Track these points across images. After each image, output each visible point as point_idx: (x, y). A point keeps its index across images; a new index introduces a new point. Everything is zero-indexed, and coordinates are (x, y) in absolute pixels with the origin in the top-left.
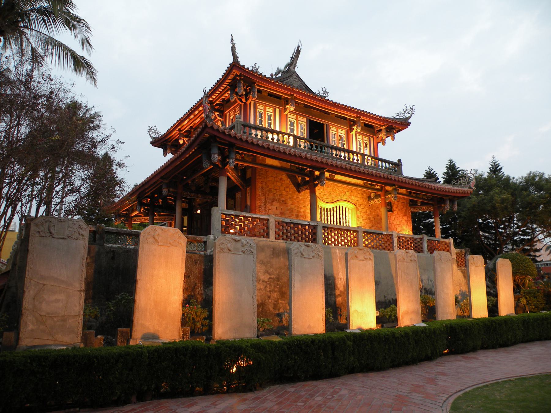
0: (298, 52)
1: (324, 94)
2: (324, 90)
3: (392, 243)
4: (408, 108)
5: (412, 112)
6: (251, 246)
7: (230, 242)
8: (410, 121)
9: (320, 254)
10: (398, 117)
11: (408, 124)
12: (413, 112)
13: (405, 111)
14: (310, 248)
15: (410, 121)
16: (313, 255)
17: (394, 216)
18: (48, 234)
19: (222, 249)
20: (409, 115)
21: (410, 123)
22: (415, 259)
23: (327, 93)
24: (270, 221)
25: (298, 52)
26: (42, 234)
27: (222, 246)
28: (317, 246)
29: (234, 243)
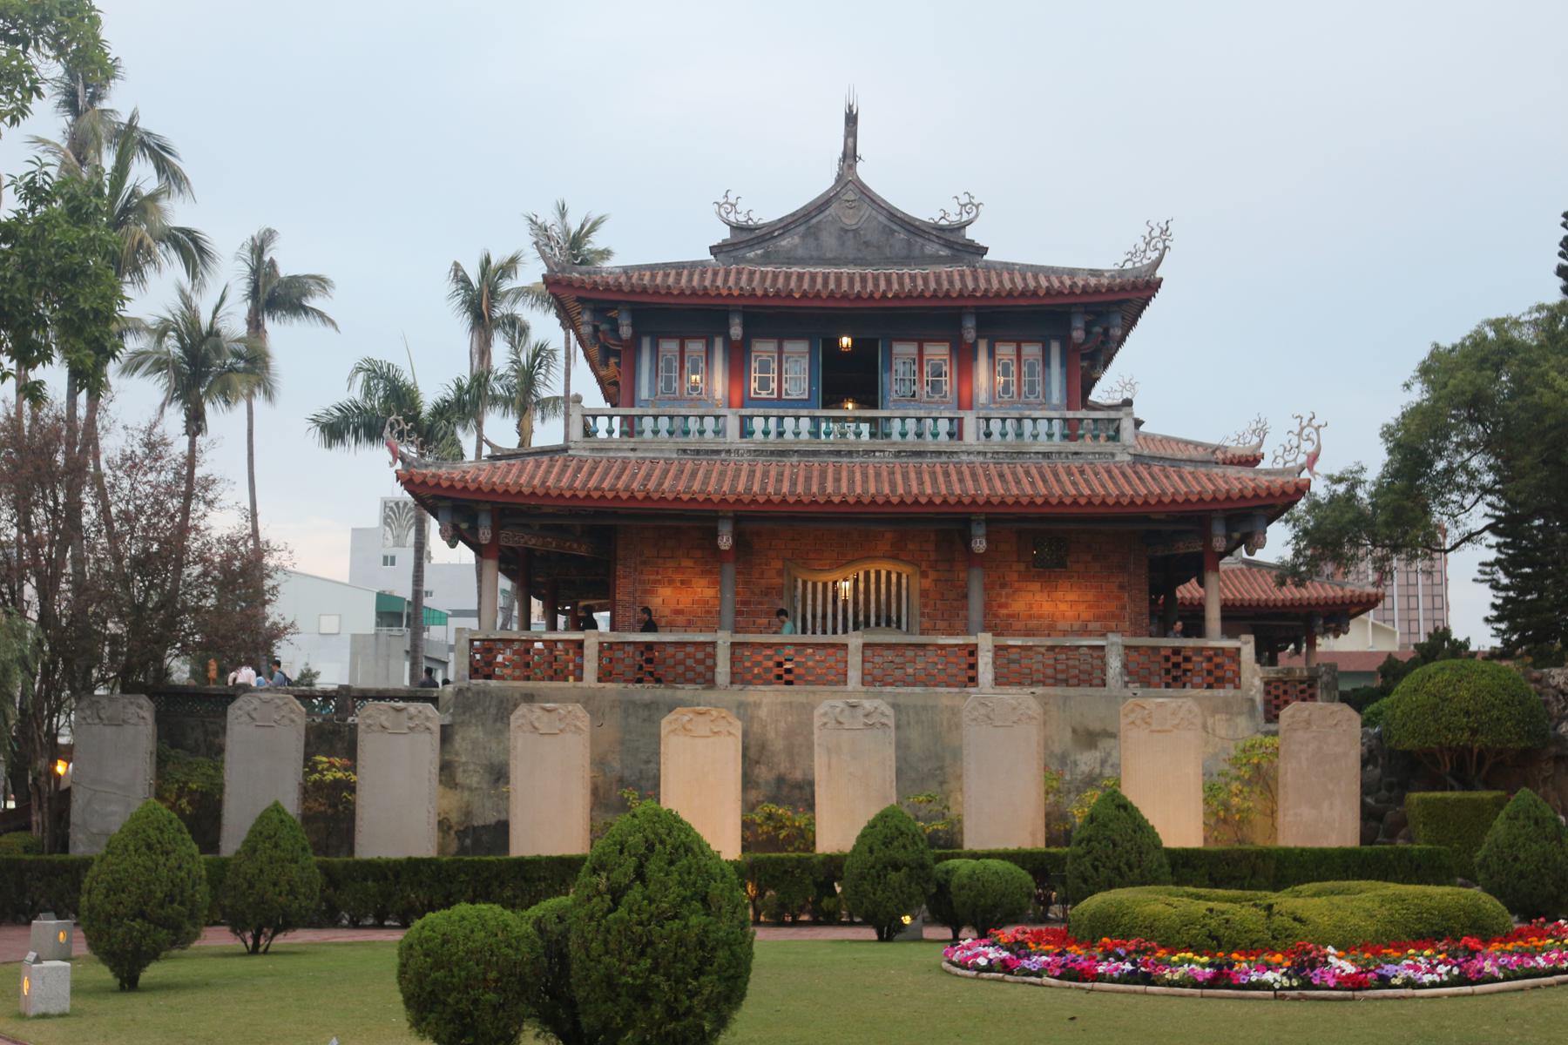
0: (851, 120)
1: (965, 214)
2: (965, 200)
3: (973, 666)
4: (1156, 233)
5: (1164, 241)
6: (428, 719)
7: (385, 712)
8: (1159, 273)
9: (578, 723)
10: (1129, 265)
11: (1159, 283)
12: (1167, 243)
13: (1148, 244)
14: (554, 715)
15: (1159, 273)
16: (562, 727)
17: (1070, 577)
18: (97, 721)
19: (369, 726)
20: (1155, 255)
21: (1161, 279)
22: (884, 720)
23: (977, 207)
24: (586, 643)
25: (851, 120)
26: (89, 720)
27: (369, 721)
28: (570, 708)
29: (392, 714)
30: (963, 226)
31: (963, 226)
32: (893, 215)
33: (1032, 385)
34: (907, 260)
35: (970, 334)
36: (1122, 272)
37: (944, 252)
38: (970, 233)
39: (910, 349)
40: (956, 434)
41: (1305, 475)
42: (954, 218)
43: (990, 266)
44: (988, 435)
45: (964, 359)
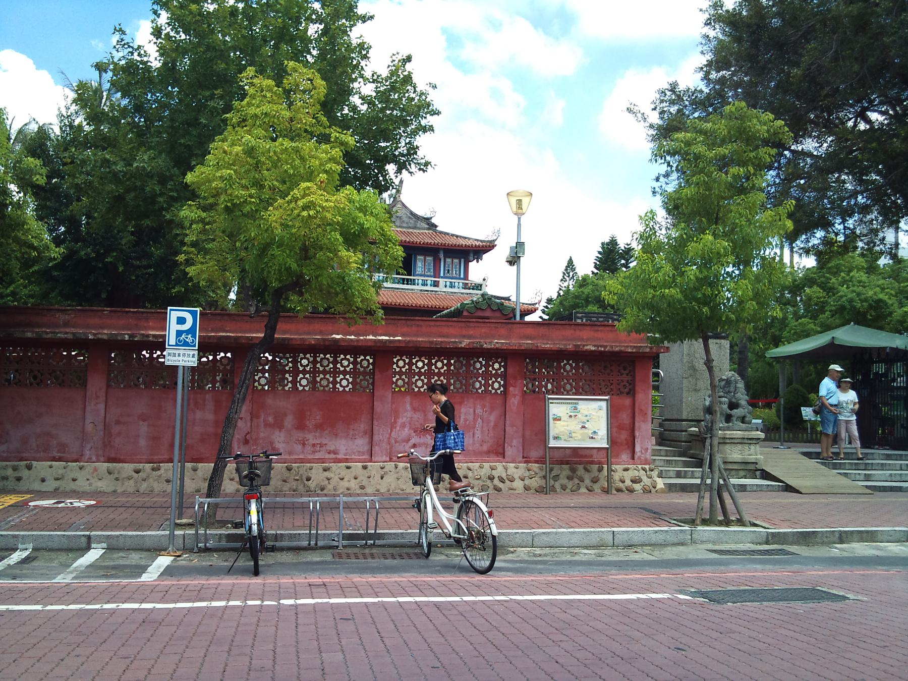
8: (496, 243)
15: (496, 243)
20: (495, 238)
30: (431, 218)
31: (431, 218)
32: (412, 213)
33: (448, 271)
34: (415, 228)
35: (442, 256)
36: (484, 241)
37: (427, 226)
38: (433, 221)
39: (422, 257)
40: (436, 284)
41: (537, 306)
42: (428, 216)
43: (441, 232)
44: (446, 286)
45: (437, 262)
